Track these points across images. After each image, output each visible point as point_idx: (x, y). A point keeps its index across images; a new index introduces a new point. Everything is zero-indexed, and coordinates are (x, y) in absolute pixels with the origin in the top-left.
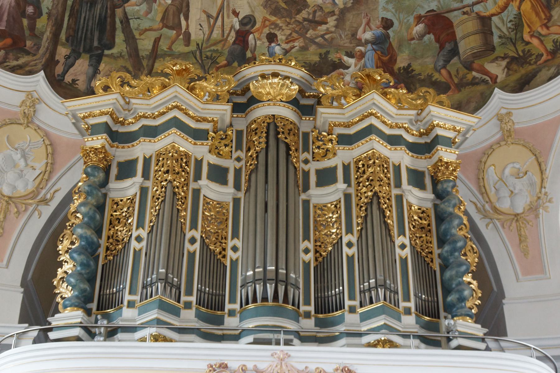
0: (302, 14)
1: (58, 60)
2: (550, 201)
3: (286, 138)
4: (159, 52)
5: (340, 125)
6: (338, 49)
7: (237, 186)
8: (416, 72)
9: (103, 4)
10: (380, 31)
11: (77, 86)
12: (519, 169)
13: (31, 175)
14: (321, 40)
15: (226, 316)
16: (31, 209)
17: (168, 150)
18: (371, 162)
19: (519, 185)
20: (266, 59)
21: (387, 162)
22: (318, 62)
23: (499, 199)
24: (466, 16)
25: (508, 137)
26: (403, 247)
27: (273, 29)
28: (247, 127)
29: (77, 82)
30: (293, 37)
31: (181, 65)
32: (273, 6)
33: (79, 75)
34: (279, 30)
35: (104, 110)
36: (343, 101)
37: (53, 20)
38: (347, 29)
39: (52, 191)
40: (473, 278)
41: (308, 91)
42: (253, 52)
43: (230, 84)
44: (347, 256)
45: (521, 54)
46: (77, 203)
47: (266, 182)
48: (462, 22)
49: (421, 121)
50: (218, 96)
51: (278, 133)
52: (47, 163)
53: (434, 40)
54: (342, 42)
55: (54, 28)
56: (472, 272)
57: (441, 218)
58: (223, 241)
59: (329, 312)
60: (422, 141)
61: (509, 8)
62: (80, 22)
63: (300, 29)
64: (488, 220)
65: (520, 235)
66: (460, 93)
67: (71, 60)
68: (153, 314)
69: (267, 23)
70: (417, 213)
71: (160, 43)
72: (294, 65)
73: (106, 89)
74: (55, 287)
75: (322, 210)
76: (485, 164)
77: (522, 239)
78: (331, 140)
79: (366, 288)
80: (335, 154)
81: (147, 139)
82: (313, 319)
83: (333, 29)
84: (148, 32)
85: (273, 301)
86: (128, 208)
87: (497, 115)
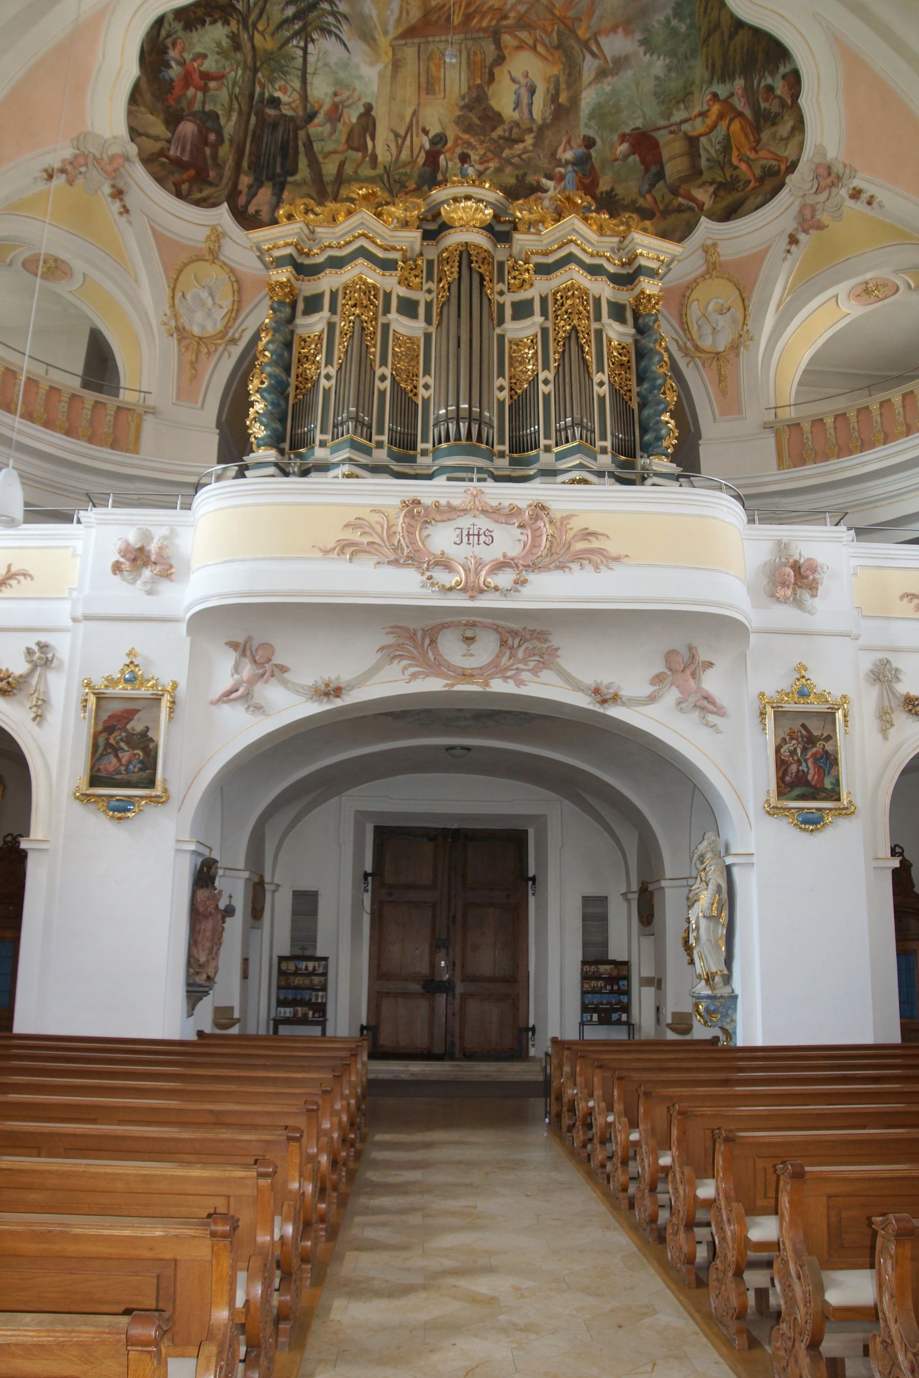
2: (751, 339)
3: (480, 267)
5: (537, 253)
7: (428, 321)
8: (620, 197)
10: (582, 150)
13: (219, 315)
15: (419, 455)
16: (221, 349)
18: (570, 294)
19: (723, 322)
21: (587, 294)
23: (701, 336)
24: (672, 136)
25: (713, 270)
26: (601, 384)
35: (289, 241)
39: (240, 330)
40: (671, 417)
42: (444, 174)
43: (419, 209)
44: (544, 393)
45: (729, 179)
46: (264, 340)
47: (459, 316)
49: (624, 249)
51: (471, 262)
52: (234, 301)
56: (671, 411)
57: (641, 354)
58: (415, 378)
60: (624, 271)
61: (718, 128)
64: (688, 359)
65: (720, 375)
68: (345, 454)
69: (460, 142)
73: (290, 217)
74: (248, 427)
75: (517, 345)
77: (721, 378)
78: (528, 270)
80: (532, 285)
81: (334, 271)
82: (507, 458)
85: (467, 440)
86: (316, 345)
87: (703, 246)
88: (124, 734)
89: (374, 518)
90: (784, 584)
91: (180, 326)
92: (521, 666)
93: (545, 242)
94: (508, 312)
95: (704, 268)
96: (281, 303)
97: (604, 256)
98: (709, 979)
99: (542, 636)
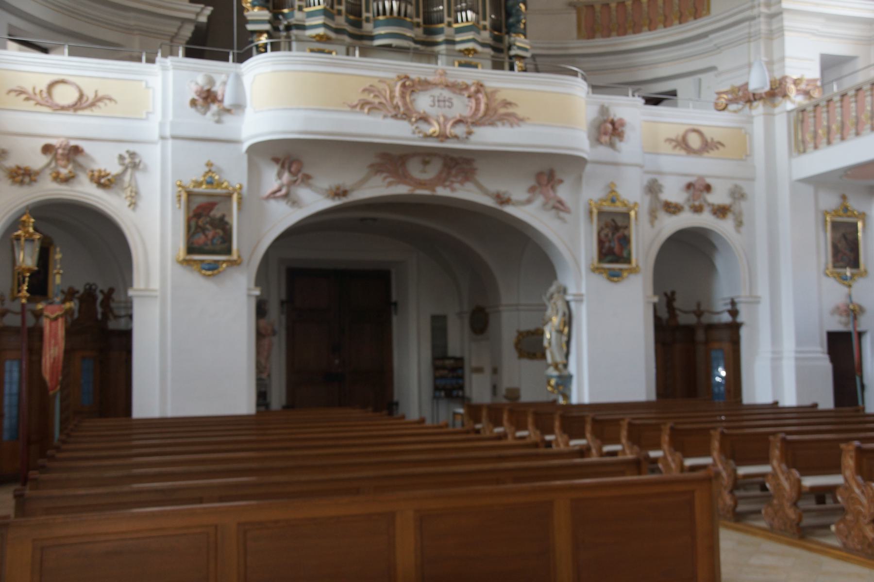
88: (208, 219)
89: (381, 86)
90: (605, 134)
92: (453, 179)
98: (556, 366)
99: (469, 161)
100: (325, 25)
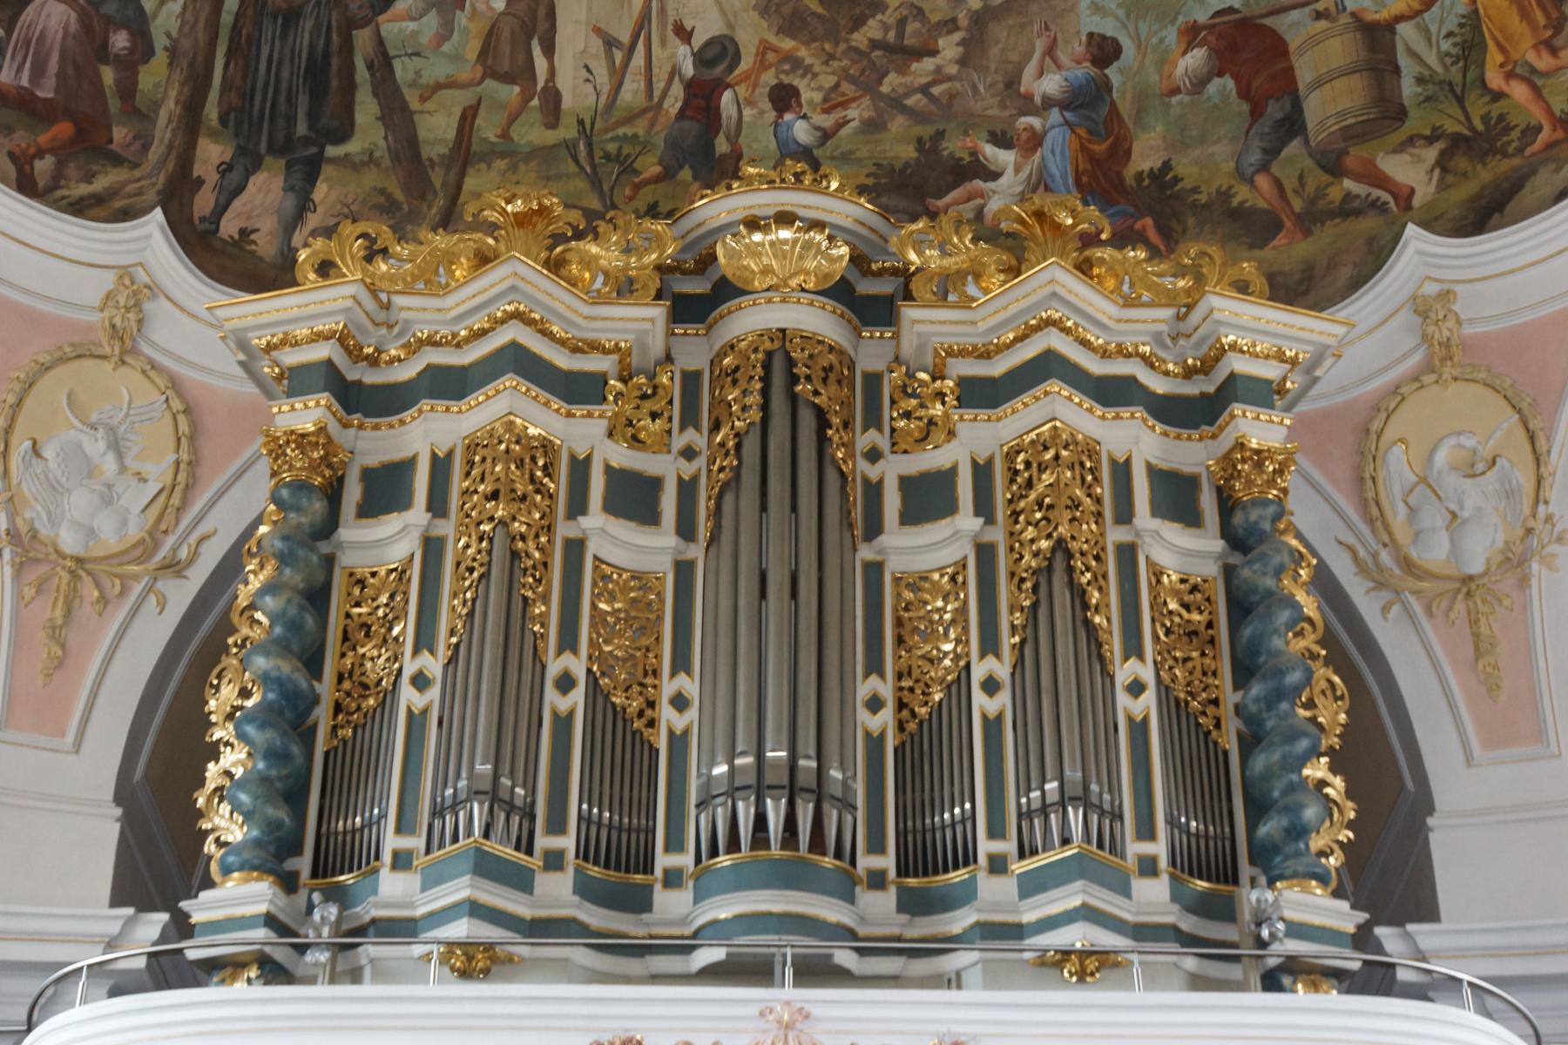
0: (865, 28)
1: (199, 177)
3: (816, 393)
4: (475, 147)
5: (962, 353)
6: (969, 123)
7: (686, 530)
8: (1187, 184)
9: (317, 18)
10: (1085, 71)
11: (253, 247)
12: (1474, 451)
13: (135, 498)
14: (920, 101)
15: (658, 887)
16: (137, 588)
17: (496, 435)
18: (1049, 455)
19: (1475, 496)
20: (760, 175)
21: (1092, 453)
22: (913, 163)
23: (1417, 535)
24: (1323, 24)
25: (1443, 360)
26: (1136, 688)
27: (787, 73)
28: (712, 361)
29: (253, 237)
30: (843, 94)
31: (527, 198)
32: (787, 10)
33: (259, 215)
34: (803, 76)
35: (320, 327)
36: (971, 289)
37: (185, 66)
38: (993, 68)
39: (193, 540)
40: (1334, 769)
41: (877, 258)
44: (985, 717)
45: (1480, 127)
46: (255, 583)
48: (1314, 41)
49: (1189, 336)
50: (631, 281)
51: (794, 379)
52: (178, 463)
53: (1234, 91)
54: (979, 104)
55: (186, 89)
56: (1330, 752)
57: (1242, 605)
58: (649, 681)
59: (936, 873)
60: (1192, 389)
62: (257, 69)
63: (863, 72)
64: (1386, 595)
65: (1476, 636)
66: (1310, 239)
67: (235, 176)
68: (460, 889)
69: (771, 56)
70: (1176, 593)
71: (478, 122)
72: (836, 190)
73: (325, 268)
74: (200, 814)
75: (913, 587)
76: (1379, 437)
77: (1480, 647)
78: (940, 395)
79: (1036, 805)
80: (951, 434)
81: (441, 405)
82: (893, 890)
83: (953, 69)
84: (444, 91)
85: (783, 847)
86: (392, 597)
87: (1414, 298)
91: (23, 529)
93: (982, 326)
94: (892, 502)
95: (1417, 358)
96: (299, 486)
97: (1138, 354)
100: (475, 909)
